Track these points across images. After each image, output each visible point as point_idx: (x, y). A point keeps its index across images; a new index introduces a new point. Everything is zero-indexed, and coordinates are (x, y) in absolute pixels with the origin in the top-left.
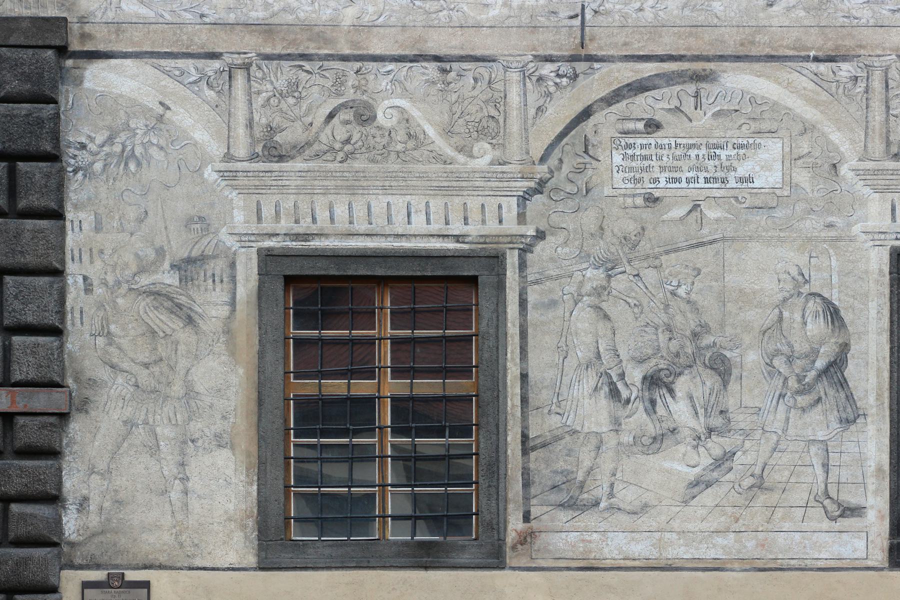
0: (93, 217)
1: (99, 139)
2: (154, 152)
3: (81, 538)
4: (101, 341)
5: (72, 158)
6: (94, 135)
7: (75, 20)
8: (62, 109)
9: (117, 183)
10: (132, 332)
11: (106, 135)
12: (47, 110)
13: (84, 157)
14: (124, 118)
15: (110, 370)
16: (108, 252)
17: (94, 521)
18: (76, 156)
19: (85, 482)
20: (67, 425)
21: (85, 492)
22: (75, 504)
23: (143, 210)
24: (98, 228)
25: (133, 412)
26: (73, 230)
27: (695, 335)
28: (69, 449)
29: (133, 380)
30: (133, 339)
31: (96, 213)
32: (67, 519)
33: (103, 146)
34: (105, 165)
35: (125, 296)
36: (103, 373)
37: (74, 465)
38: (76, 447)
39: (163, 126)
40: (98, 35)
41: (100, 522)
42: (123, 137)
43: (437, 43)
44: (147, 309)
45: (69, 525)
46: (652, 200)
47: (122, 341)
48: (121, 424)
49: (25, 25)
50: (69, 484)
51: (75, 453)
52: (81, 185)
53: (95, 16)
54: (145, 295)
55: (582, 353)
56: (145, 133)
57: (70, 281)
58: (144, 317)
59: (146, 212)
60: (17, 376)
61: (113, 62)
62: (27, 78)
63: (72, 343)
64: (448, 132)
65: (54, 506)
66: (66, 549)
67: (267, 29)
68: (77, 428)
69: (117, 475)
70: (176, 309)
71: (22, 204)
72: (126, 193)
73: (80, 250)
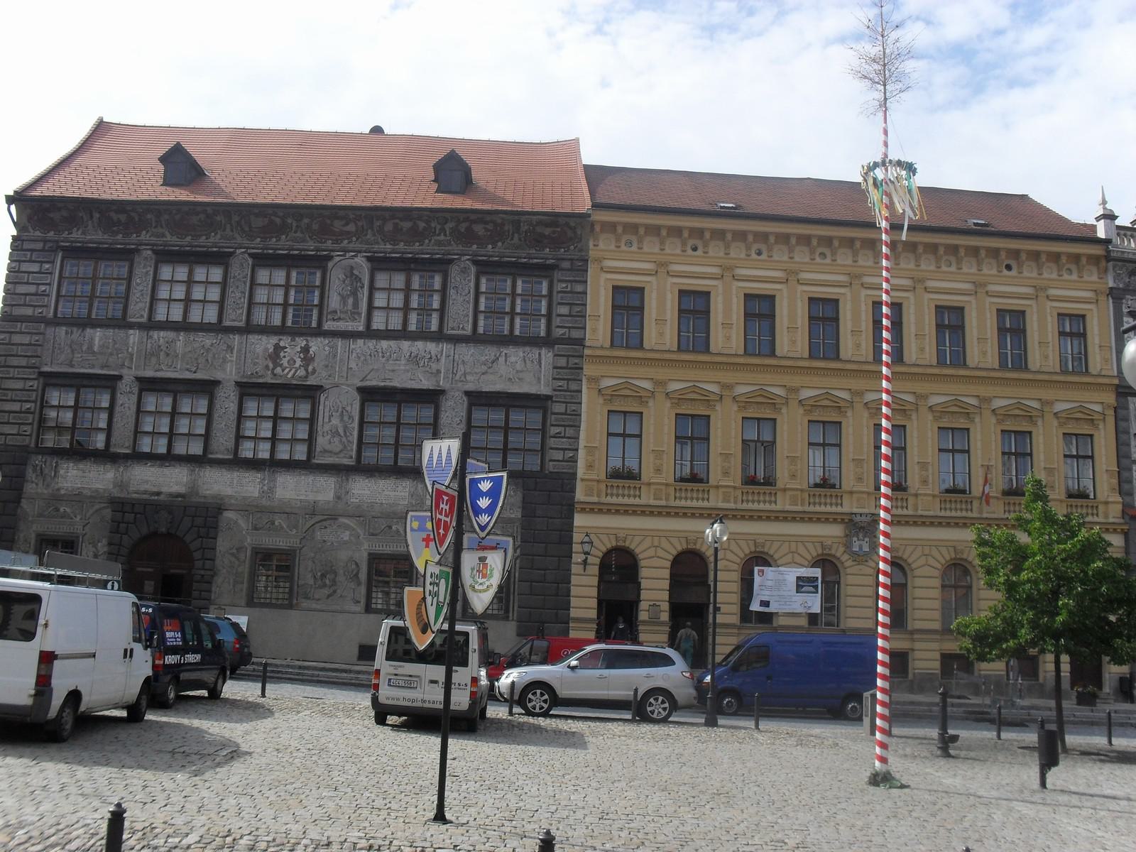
27: (332, 567)
43: (288, 510)
46: (325, 541)
50: (213, 589)
55: (309, 569)
64: (288, 527)
67: (257, 506)
70: (236, 557)
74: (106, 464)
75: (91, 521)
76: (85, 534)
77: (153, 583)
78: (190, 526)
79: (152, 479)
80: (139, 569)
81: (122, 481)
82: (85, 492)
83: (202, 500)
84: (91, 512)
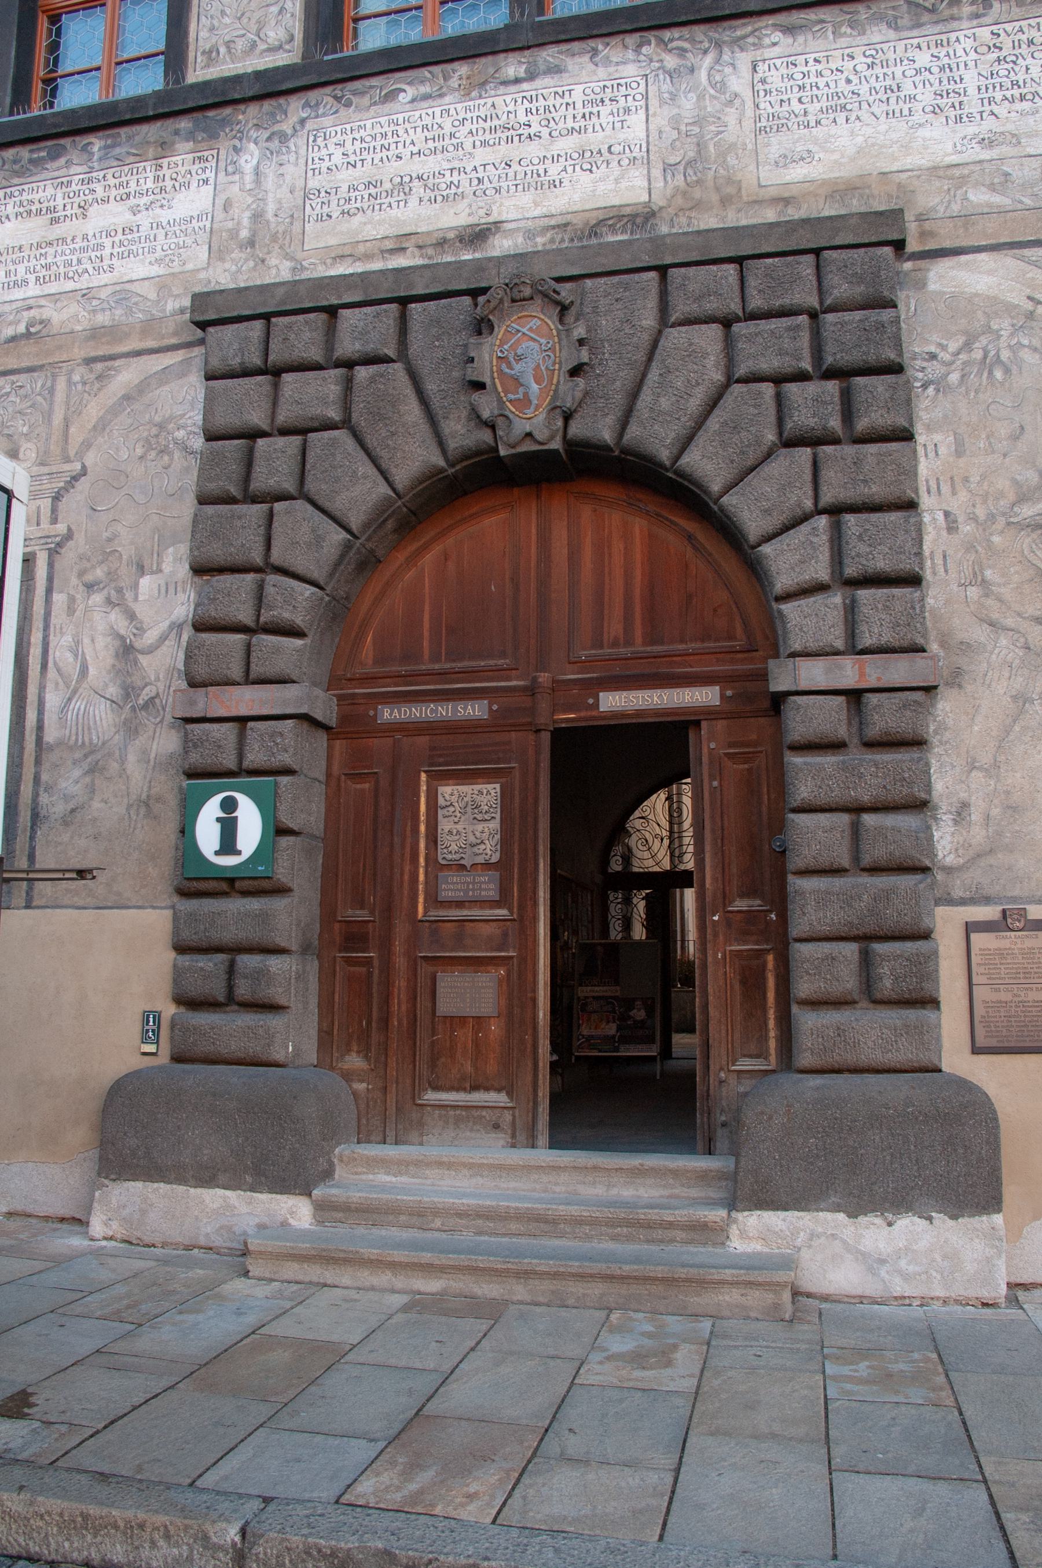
0: (952, 438)
1: (953, 346)
2: (1026, 355)
3: (962, 861)
4: (973, 592)
5: (917, 372)
6: (945, 343)
7: (913, 219)
8: (903, 317)
9: (981, 395)
10: (1016, 578)
11: (961, 341)
12: (886, 315)
13: (934, 370)
14: (982, 319)
15: (989, 629)
16: (975, 479)
17: (978, 835)
18: (924, 368)
19: (963, 782)
20: (933, 706)
21: (963, 795)
22: (951, 813)
23: (1017, 425)
24: (959, 453)
25: (1024, 684)
26: (926, 455)
28: (939, 737)
29: (1022, 640)
30: (1017, 588)
31: (955, 434)
32: (940, 834)
33: (958, 354)
34: (963, 376)
35: (1002, 532)
36: (979, 634)
37: (947, 759)
38: (947, 735)
39: (1034, 324)
40: (942, 231)
41: (988, 837)
42: (984, 340)
44: (1034, 546)
45: (943, 842)
47: (1002, 590)
48: (1009, 699)
49: (853, 221)
50: (939, 786)
51: (946, 742)
52: (934, 399)
53: (936, 211)
54: (1029, 530)
56: (1012, 335)
57: (927, 518)
58: (1031, 557)
59: (1022, 428)
60: (867, 640)
61: (963, 258)
62: (860, 279)
63: (934, 597)
65: (922, 816)
66: (940, 877)
68: (948, 709)
69: (1007, 771)
71: (862, 424)
72: (993, 406)
73: (938, 479)
74: (165, 148)
75: (90, 459)
76: (69, 535)
77: (488, 793)
78: (718, 377)
79: (430, 165)
80: (388, 714)
81: (257, 217)
82: (57, 316)
83: (770, 215)
84: (93, 411)
